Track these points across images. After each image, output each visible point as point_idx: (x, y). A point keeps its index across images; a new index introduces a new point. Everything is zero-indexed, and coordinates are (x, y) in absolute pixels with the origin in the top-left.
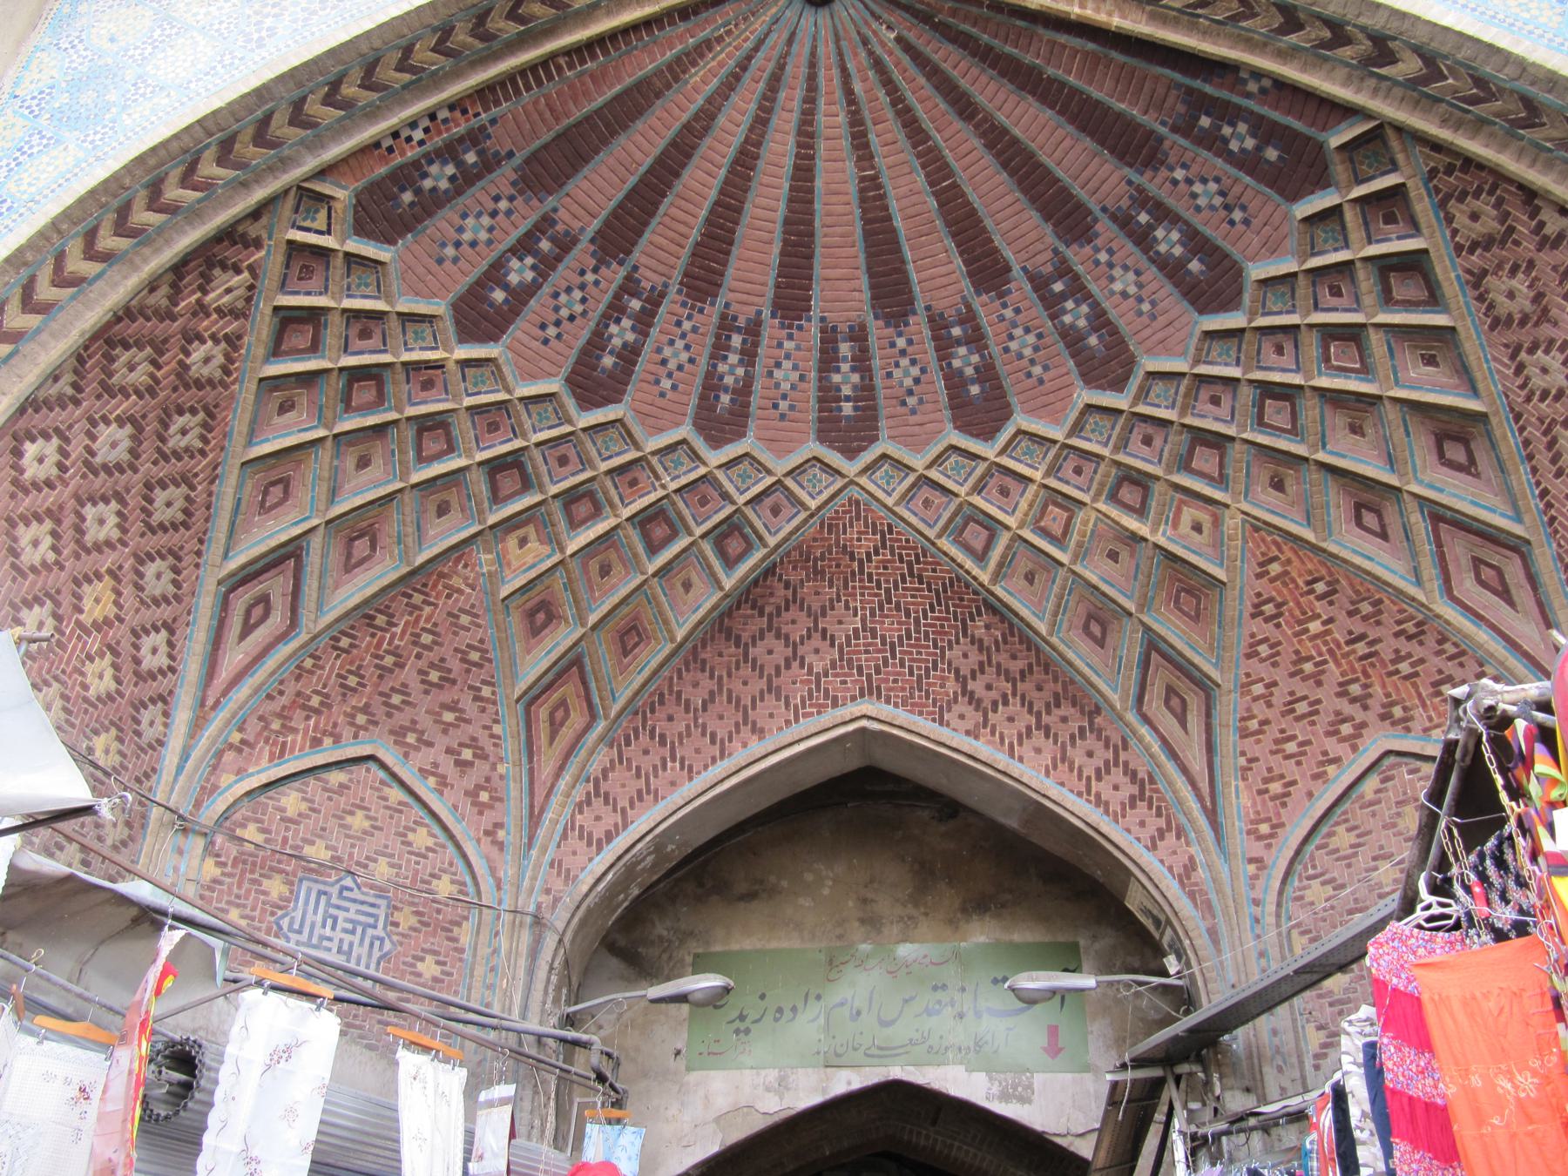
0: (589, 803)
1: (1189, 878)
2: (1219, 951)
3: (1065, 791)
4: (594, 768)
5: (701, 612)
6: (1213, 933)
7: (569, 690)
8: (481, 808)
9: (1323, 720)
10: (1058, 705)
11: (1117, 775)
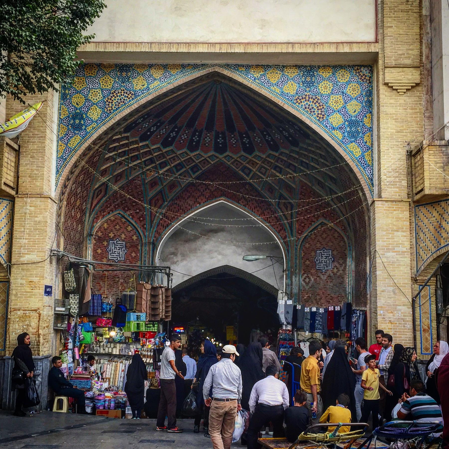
8: (141, 221)
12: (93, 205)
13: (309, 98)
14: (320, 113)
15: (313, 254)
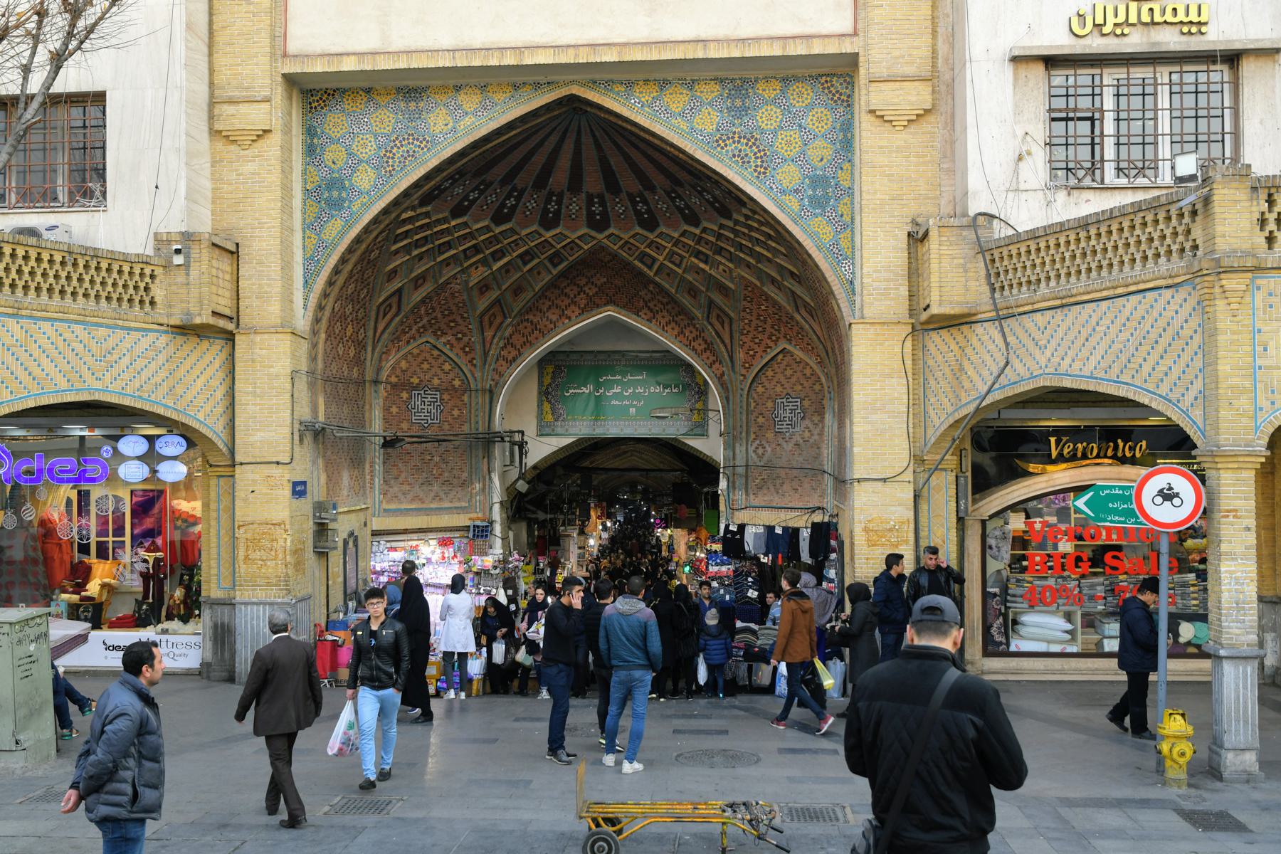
4: (507, 334)
5: (544, 282)
7: (496, 310)
8: (466, 353)
9: (767, 334)
11: (700, 341)
12: (379, 331)
13: (740, 137)
14: (759, 163)
15: (770, 404)
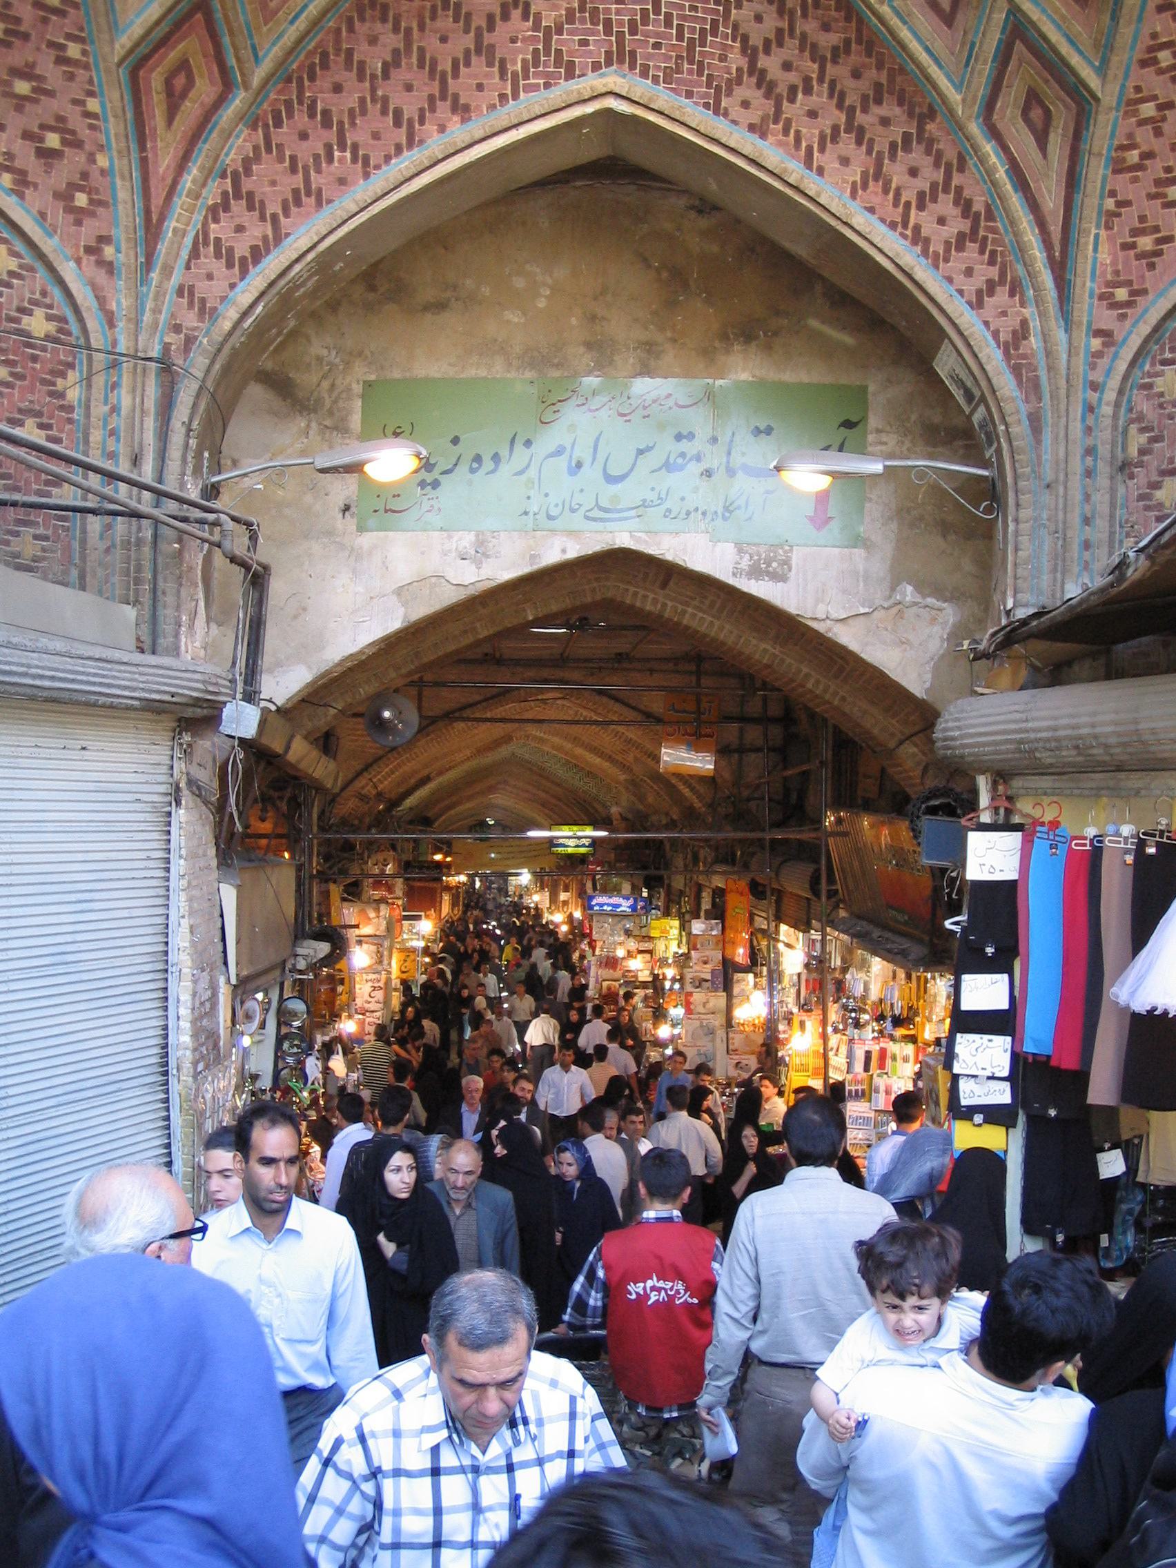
0: (227, 208)
1: (1017, 348)
2: (1038, 441)
3: (873, 219)
4: (232, 157)
6: (1035, 422)
10: (879, 101)
11: (946, 205)
